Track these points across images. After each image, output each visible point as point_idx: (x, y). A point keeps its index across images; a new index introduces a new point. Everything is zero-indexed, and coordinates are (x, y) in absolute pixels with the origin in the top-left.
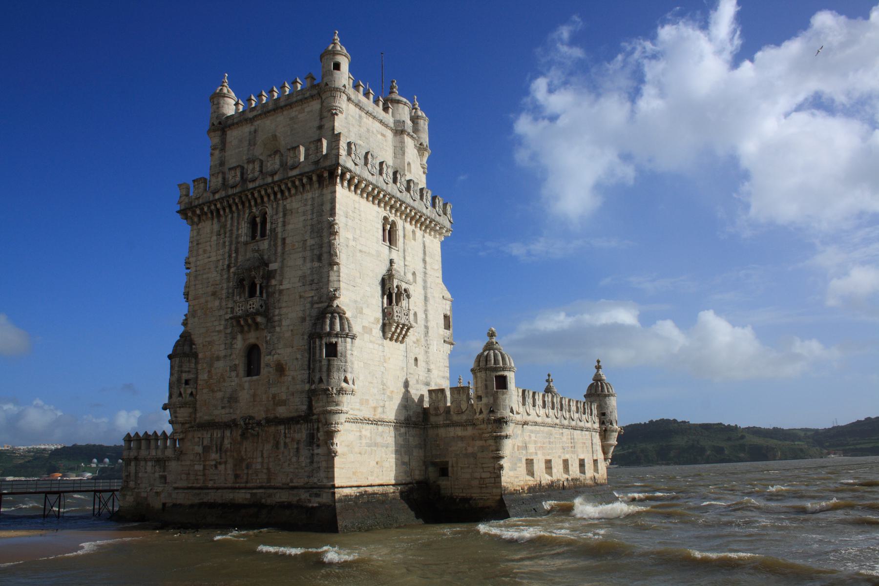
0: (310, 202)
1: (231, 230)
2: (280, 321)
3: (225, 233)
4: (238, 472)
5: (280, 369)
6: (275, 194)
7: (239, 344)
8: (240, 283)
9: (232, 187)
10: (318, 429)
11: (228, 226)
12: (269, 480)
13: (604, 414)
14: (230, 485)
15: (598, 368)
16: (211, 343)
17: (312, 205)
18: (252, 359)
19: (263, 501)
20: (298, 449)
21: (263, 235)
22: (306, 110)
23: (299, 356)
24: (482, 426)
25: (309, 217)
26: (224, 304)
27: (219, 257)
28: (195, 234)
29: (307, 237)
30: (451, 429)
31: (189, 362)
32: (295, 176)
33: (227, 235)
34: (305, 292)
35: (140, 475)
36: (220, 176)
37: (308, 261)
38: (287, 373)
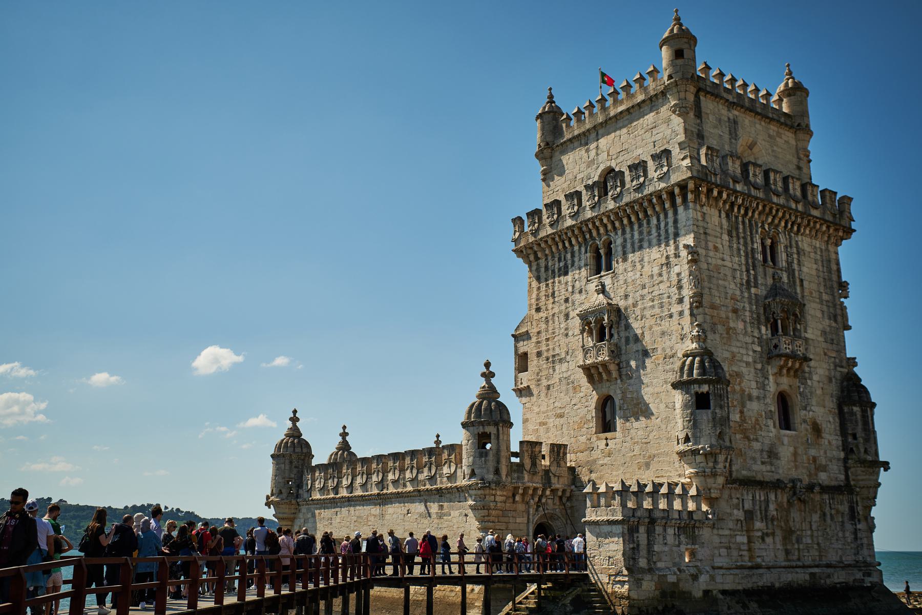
0: (819, 253)
1: (744, 238)
2: (810, 373)
3: (738, 238)
4: (789, 547)
5: (817, 429)
9: (755, 188)
11: (741, 231)
14: (787, 563)
17: (821, 256)
19: (822, 581)
23: (831, 419)
26: (749, 329)
33: (742, 241)
35: (656, 548)
38: (823, 435)
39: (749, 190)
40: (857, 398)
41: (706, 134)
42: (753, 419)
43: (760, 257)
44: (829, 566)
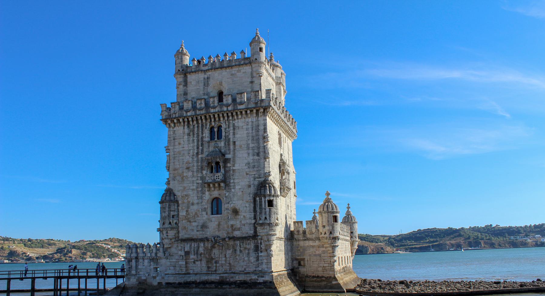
0: (250, 124)
2: (234, 186)
3: (194, 134)
5: (236, 212)
6: (228, 117)
7: (207, 196)
8: (209, 163)
10: (261, 243)
12: (230, 269)
13: (352, 233)
15: (349, 208)
16: (186, 195)
17: (252, 125)
18: (216, 206)
20: (249, 253)
21: (219, 137)
22: (242, 71)
23: (247, 205)
24: (326, 241)
25: (250, 132)
26: (195, 174)
27: (191, 148)
28: (172, 133)
29: (250, 142)
30: (307, 242)
31: (174, 205)
32: (243, 109)
33: (195, 136)
34: (250, 171)
35: (139, 267)
36: (190, 102)
37: (251, 155)
38: (240, 214)
39: (195, 113)
40: (259, 193)
41: (189, 92)
42: (194, 213)
43: (207, 139)
44: (234, 273)
